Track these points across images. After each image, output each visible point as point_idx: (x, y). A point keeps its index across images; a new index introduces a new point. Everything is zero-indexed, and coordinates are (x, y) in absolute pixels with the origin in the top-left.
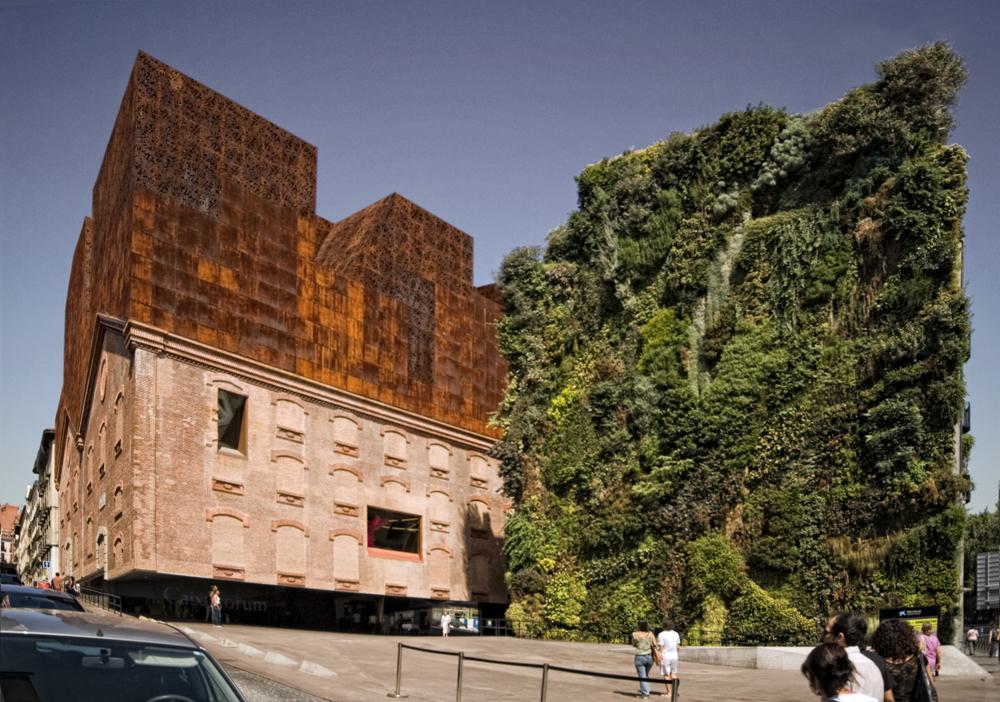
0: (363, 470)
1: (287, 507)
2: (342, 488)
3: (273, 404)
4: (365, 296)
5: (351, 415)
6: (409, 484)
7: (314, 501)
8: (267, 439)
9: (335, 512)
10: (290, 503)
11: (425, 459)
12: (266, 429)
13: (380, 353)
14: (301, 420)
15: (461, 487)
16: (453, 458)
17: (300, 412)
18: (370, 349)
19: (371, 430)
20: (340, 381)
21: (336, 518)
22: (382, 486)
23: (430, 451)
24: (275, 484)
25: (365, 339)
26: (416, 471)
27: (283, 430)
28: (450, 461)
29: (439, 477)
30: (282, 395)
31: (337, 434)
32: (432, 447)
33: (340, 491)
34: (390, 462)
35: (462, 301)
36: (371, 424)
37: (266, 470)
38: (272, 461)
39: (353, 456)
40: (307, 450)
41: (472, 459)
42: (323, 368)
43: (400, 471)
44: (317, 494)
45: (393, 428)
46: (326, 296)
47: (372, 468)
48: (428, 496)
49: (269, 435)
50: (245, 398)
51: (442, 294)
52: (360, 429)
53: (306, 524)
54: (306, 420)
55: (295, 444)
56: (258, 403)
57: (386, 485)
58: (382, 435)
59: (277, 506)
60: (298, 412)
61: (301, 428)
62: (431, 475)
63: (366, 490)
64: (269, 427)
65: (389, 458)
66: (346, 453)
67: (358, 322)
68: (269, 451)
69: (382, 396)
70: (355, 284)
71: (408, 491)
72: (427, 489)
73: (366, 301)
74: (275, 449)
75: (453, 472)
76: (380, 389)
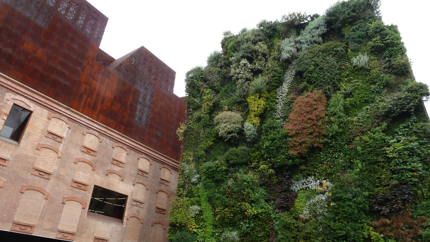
1: (37, 178)
2: (81, 173)
3: (49, 119)
5: (97, 134)
7: (59, 177)
8: (38, 136)
9: (71, 186)
10: (41, 176)
12: (39, 131)
14: (64, 131)
15: (154, 183)
16: (152, 167)
17: (65, 126)
21: (72, 190)
22: (107, 175)
23: (140, 161)
24: (34, 163)
26: (129, 169)
27: (50, 133)
28: (150, 167)
30: (57, 115)
31: (86, 142)
32: (141, 159)
33: (79, 174)
34: (115, 162)
36: (108, 141)
37: (31, 154)
38: (37, 149)
39: (92, 155)
40: (63, 147)
41: (162, 168)
42: (86, 108)
43: (119, 168)
44: (63, 174)
45: (120, 145)
47: (103, 164)
48: (134, 185)
49: (40, 135)
50: (31, 112)
52: (101, 142)
53: (48, 190)
54: (68, 132)
55: (56, 142)
56: (39, 117)
57: (110, 175)
58: (113, 148)
59: (31, 177)
60: (64, 126)
61: (64, 135)
62: (138, 174)
63: (96, 175)
64: (42, 130)
66: (88, 153)
68: (37, 143)
71: (122, 180)
72: (134, 181)
74: (42, 143)
75: (151, 174)
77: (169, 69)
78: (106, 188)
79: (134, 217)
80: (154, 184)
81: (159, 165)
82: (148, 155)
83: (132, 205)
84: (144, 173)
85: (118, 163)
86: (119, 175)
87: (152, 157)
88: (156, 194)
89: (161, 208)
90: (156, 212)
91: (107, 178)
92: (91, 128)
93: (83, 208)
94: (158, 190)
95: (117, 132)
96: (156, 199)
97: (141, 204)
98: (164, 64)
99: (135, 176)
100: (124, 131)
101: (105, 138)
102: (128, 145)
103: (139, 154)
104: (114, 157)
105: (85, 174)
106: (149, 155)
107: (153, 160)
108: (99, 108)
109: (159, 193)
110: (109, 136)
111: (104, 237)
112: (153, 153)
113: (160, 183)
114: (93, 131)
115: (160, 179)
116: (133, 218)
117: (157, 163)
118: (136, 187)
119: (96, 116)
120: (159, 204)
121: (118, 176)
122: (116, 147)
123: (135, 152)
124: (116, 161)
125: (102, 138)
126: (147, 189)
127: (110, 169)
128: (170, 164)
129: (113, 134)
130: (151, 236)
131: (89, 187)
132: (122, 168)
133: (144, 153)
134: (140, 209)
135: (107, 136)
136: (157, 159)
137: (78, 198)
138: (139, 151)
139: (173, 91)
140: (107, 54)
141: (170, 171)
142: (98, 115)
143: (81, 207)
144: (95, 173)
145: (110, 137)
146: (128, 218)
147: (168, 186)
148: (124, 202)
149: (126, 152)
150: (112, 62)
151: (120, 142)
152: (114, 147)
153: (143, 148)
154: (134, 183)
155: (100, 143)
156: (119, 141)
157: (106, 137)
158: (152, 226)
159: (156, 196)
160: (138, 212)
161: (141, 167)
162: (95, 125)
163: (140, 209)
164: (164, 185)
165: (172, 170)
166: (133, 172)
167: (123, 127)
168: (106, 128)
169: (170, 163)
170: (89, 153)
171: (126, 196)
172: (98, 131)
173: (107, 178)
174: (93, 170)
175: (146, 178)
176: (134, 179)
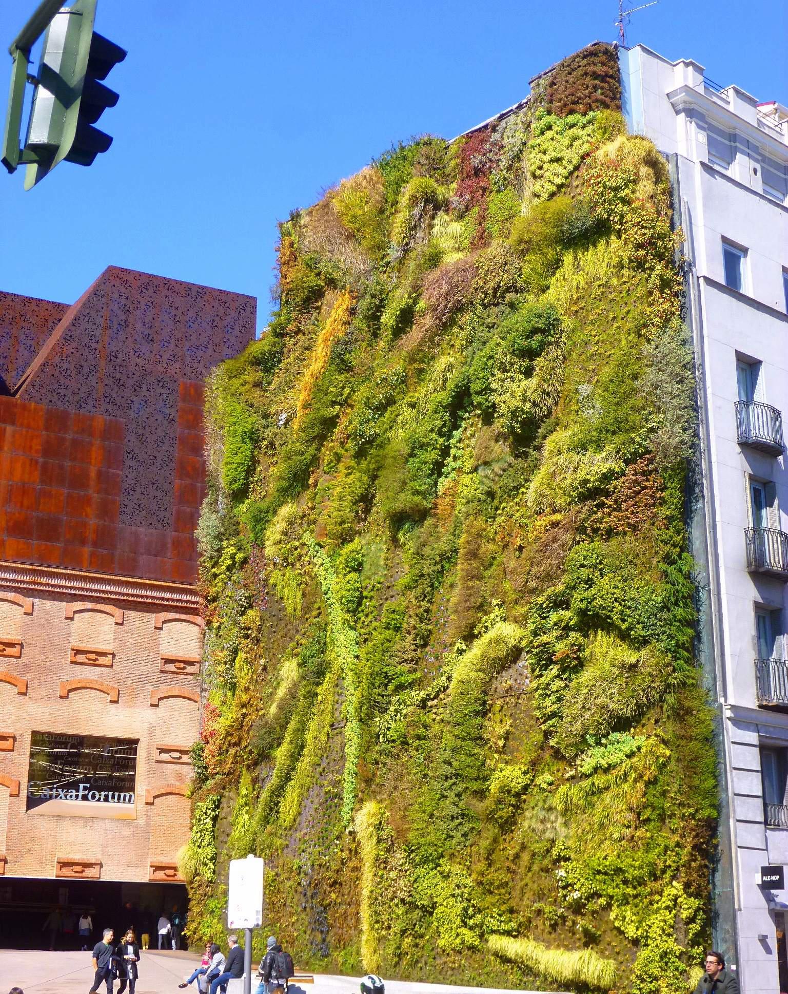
29: (180, 672)
45: (89, 605)
47: (46, 670)
62: (162, 672)
65: (78, 652)
83: (158, 762)
93: (11, 795)
100: (91, 563)
111: (85, 857)
125: (29, 600)
149: (112, 620)
161: (169, 649)
166: (144, 669)
167: (87, 550)
171: (136, 741)
176: (151, 688)
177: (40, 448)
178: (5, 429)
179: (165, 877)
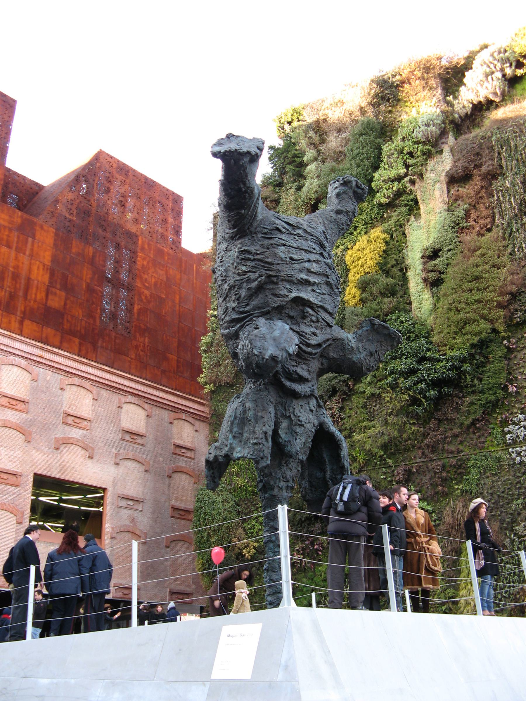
0: (33, 429)
4: (55, 240)
5: (24, 363)
6: (93, 449)
11: (117, 419)
13: (66, 299)
15: (161, 455)
16: (151, 420)
18: (55, 294)
19: (48, 382)
20: (15, 325)
22: (57, 449)
23: (123, 411)
25: (50, 282)
28: (146, 423)
32: (125, 406)
34: (70, 420)
35: (169, 254)
36: (49, 375)
39: (21, 411)
41: (176, 422)
43: (81, 432)
45: (77, 381)
46: (8, 236)
48: (117, 464)
51: (146, 246)
57: (62, 448)
58: (62, 389)
62: (122, 439)
63: (34, 453)
66: (11, 407)
67: (44, 265)
69: (65, 345)
70: (45, 228)
71: (91, 457)
72: (116, 455)
73: (55, 245)
75: (151, 437)
76: (62, 337)
77: (166, 192)
78: (57, 476)
79: (125, 533)
80: (161, 459)
81: (166, 415)
82: (139, 395)
83: (119, 507)
84: (135, 437)
85: (77, 420)
86: (82, 445)
87: (148, 398)
88: (167, 479)
89: (182, 508)
90: (172, 517)
91: (59, 455)
92: (10, 352)
93: (18, 523)
94: (171, 471)
95: (65, 353)
96: (169, 490)
97: (137, 502)
98: (154, 182)
99: (117, 444)
100: (80, 350)
101: (42, 370)
102: (93, 380)
103: (120, 396)
104: (68, 410)
105: (12, 453)
106: (142, 396)
107: (151, 406)
108: (20, 306)
109: (173, 475)
110: (49, 366)
112: (150, 391)
113: (174, 453)
114: (15, 360)
115: (172, 447)
116: (123, 533)
117: (163, 411)
118: (121, 469)
119: (17, 325)
120: (177, 499)
121: (80, 449)
122: (69, 386)
123: (110, 393)
124: (73, 418)
126: (146, 471)
127: (62, 436)
128: (191, 411)
129: (57, 359)
130: (168, 568)
131: (23, 479)
132: (87, 430)
133: (129, 392)
134: (136, 514)
135: (45, 364)
136: (160, 402)
137: (4, 504)
138: (120, 389)
139: (180, 243)
140: (24, 178)
141: (193, 425)
142: (21, 323)
143: (13, 519)
144: (32, 448)
145: (53, 367)
146: (114, 535)
147: (192, 459)
148: (100, 501)
149: (90, 396)
150: (37, 193)
151: (75, 374)
152: (65, 387)
153: (126, 383)
154: (118, 461)
155: (32, 382)
156: (72, 373)
157: (43, 367)
158: (167, 547)
159: (167, 483)
160: (133, 520)
162: (17, 345)
163: (136, 515)
164: (182, 458)
165: (197, 424)
166: (111, 436)
168: (42, 349)
169: (190, 408)
170: (13, 407)
171: (104, 490)
172: (26, 358)
173: (59, 455)
174: (28, 441)
175: (141, 447)
176: (115, 451)
177: (50, 259)
178: (27, 239)
179: (122, 595)
